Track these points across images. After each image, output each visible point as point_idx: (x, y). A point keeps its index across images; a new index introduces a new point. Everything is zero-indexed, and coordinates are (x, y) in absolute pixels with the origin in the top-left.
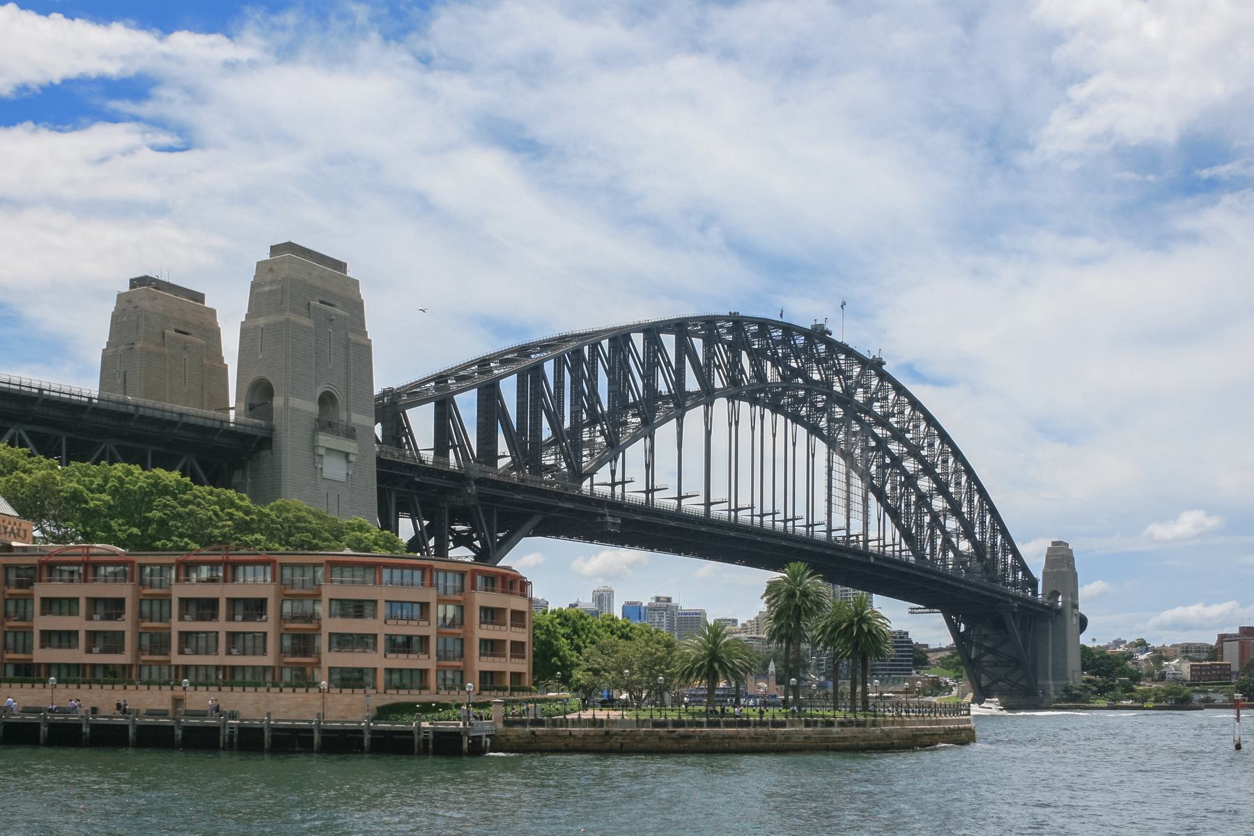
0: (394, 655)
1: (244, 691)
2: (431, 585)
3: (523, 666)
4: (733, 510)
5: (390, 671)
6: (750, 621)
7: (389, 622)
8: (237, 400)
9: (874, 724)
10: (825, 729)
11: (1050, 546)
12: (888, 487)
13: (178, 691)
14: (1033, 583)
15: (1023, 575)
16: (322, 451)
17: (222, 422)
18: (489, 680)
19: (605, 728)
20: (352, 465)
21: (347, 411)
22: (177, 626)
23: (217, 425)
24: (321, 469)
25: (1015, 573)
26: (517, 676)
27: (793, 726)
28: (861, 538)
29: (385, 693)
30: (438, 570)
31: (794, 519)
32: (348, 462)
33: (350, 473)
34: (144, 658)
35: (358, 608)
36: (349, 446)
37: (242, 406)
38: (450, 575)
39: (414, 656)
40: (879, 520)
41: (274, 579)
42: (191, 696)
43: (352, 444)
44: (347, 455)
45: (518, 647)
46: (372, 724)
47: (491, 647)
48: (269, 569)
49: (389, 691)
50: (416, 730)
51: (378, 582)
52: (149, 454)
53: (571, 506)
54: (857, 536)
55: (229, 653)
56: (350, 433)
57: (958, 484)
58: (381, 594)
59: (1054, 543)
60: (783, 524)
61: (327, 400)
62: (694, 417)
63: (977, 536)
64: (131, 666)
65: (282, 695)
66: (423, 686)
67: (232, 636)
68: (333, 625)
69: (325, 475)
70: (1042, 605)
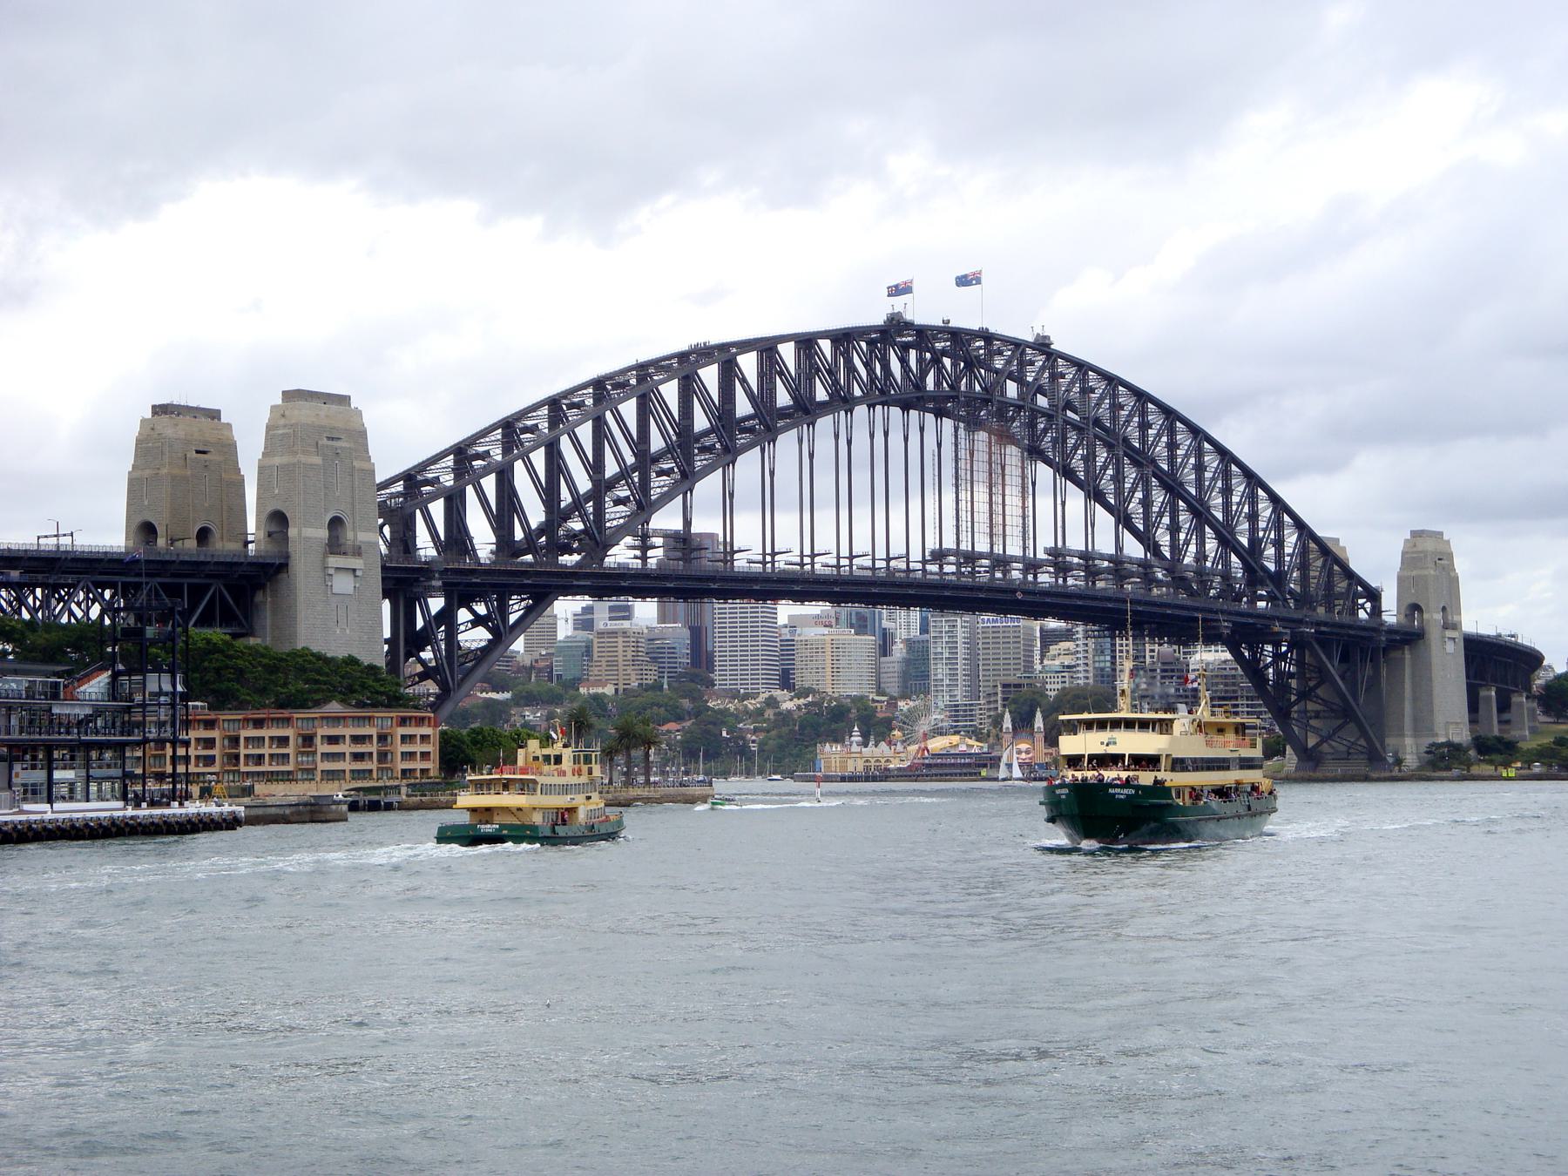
5: (352, 771)
8: (258, 528)
14: (1374, 595)
16: (331, 571)
26: (424, 771)
32: (355, 576)
37: (262, 534)
44: (354, 570)
45: (425, 755)
52: (186, 586)
53: (589, 583)
55: (270, 765)
56: (357, 552)
59: (1416, 534)
61: (336, 523)
67: (271, 756)
68: (323, 748)
70: (1392, 630)
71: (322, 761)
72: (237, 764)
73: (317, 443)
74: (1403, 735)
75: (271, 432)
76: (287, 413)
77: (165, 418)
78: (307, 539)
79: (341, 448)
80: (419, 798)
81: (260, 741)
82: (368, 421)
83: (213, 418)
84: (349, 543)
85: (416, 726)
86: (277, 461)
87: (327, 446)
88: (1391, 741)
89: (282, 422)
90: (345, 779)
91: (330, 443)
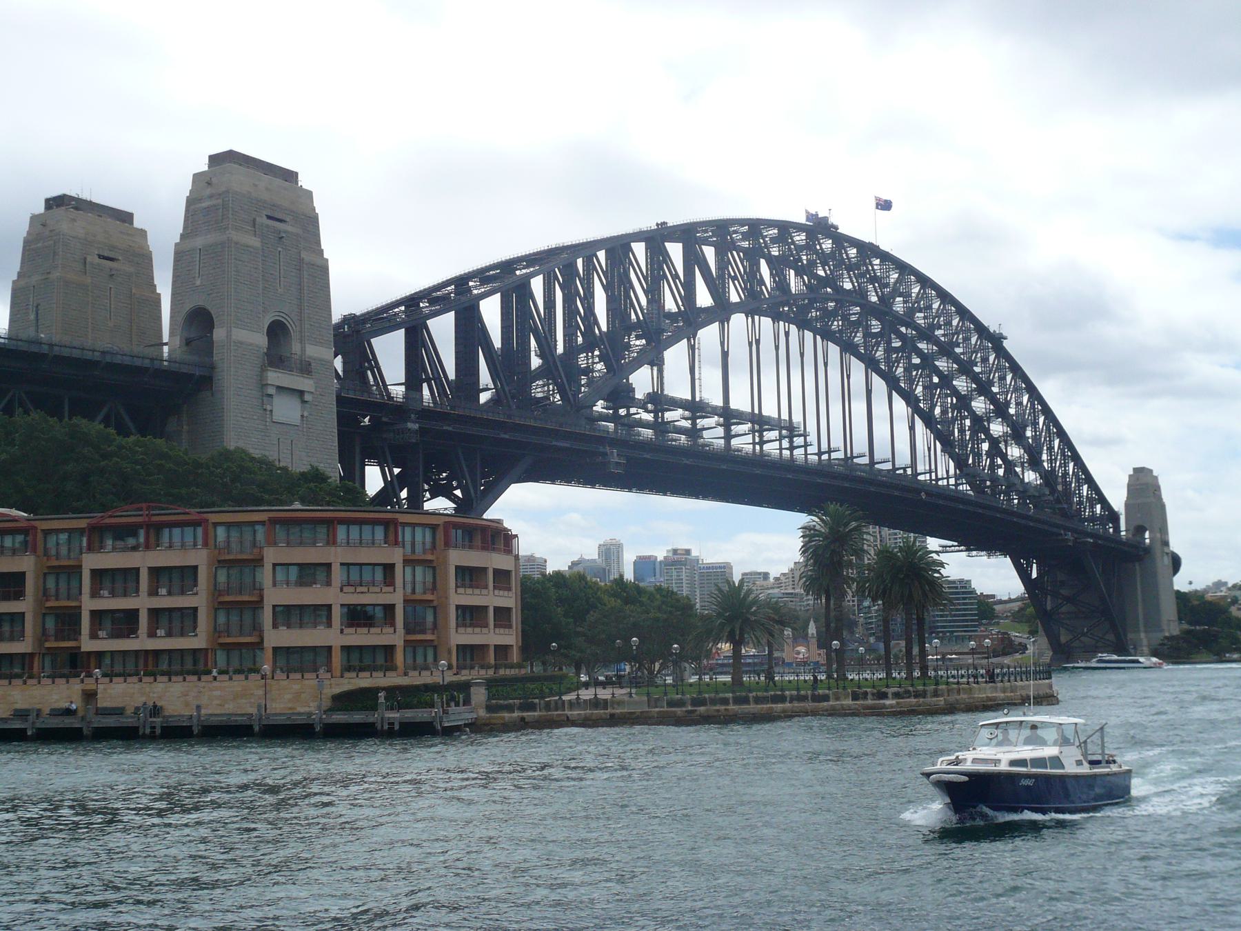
0: (352, 630)
1: (170, 680)
2: (396, 543)
3: (510, 638)
4: (757, 443)
5: (347, 649)
6: (784, 574)
7: (345, 589)
8: (172, 334)
9: (936, 694)
10: (877, 702)
11: (1132, 473)
12: (937, 411)
13: (90, 684)
14: (1113, 516)
15: (1102, 508)
16: (271, 391)
17: (152, 359)
18: (470, 653)
19: (610, 711)
20: (307, 405)
21: (301, 343)
22: (88, 604)
23: (147, 363)
24: (271, 411)
25: (1092, 507)
26: (502, 650)
27: (837, 699)
28: (909, 471)
29: (342, 677)
30: (405, 524)
31: (829, 451)
32: (304, 402)
33: (306, 414)
34: (47, 645)
35: (309, 573)
36: (305, 384)
37: (177, 341)
38: (419, 531)
39: (377, 630)
40: (929, 449)
41: (206, 544)
42: (105, 689)
43: (306, 381)
44: (301, 393)
45: (502, 614)
46: (324, 716)
47: (471, 615)
48: (200, 530)
49: (347, 675)
50: (379, 722)
51: (332, 541)
52: (66, 401)
53: (568, 445)
54: (905, 469)
55: (152, 634)
56: (305, 368)
57: (1019, 404)
58: (336, 556)
59: (1135, 469)
60: (816, 457)
61: (277, 331)
62: (708, 335)
63: (1045, 464)
64: (32, 655)
65: (216, 684)
66: (389, 667)
67: (155, 613)
68: (276, 596)
69: (275, 418)
71: (275, 626)
72: (76, 633)
73: (254, 220)
74: (1138, 631)
75: (192, 207)
76: (214, 180)
77: (61, 211)
78: (240, 343)
79: (285, 232)
80: (516, 714)
81: (124, 579)
82: (320, 205)
83: (124, 221)
84: (296, 357)
85: (484, 548)
86: (199, 242)
87: (267, 226)
88: (1130, 636)
89: (208, 191)
90: (329, 670)
91: (271, 222)
